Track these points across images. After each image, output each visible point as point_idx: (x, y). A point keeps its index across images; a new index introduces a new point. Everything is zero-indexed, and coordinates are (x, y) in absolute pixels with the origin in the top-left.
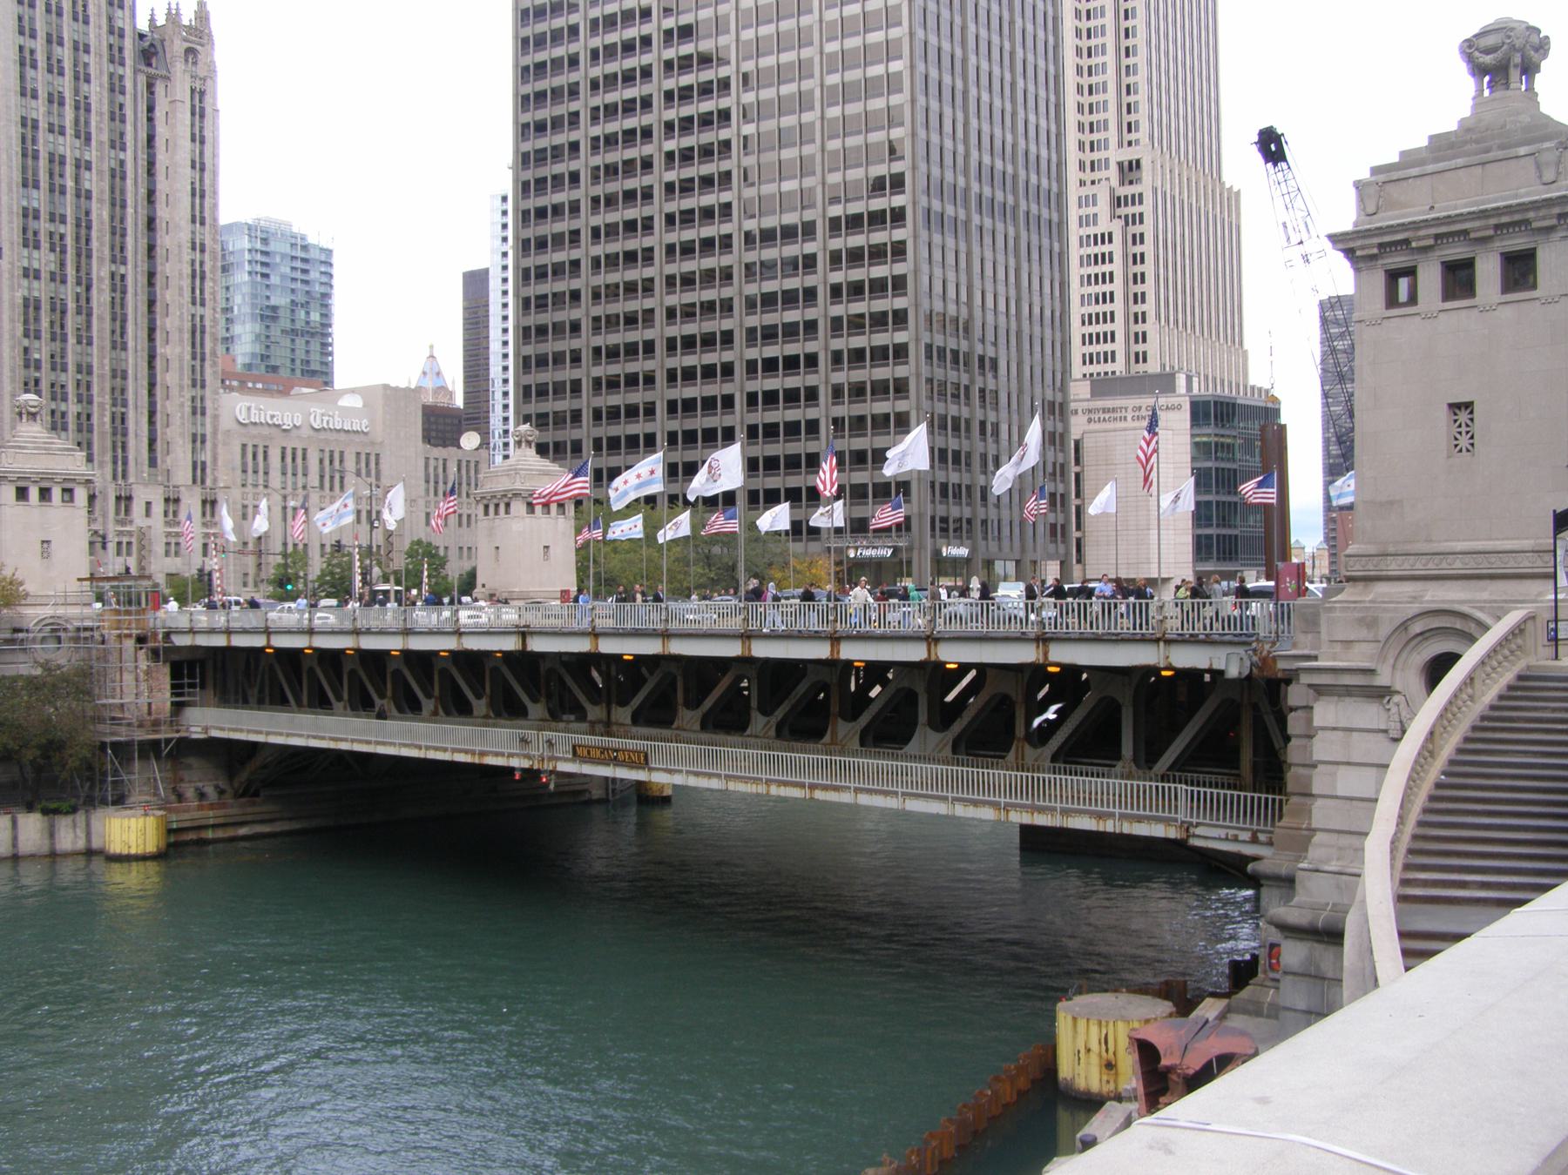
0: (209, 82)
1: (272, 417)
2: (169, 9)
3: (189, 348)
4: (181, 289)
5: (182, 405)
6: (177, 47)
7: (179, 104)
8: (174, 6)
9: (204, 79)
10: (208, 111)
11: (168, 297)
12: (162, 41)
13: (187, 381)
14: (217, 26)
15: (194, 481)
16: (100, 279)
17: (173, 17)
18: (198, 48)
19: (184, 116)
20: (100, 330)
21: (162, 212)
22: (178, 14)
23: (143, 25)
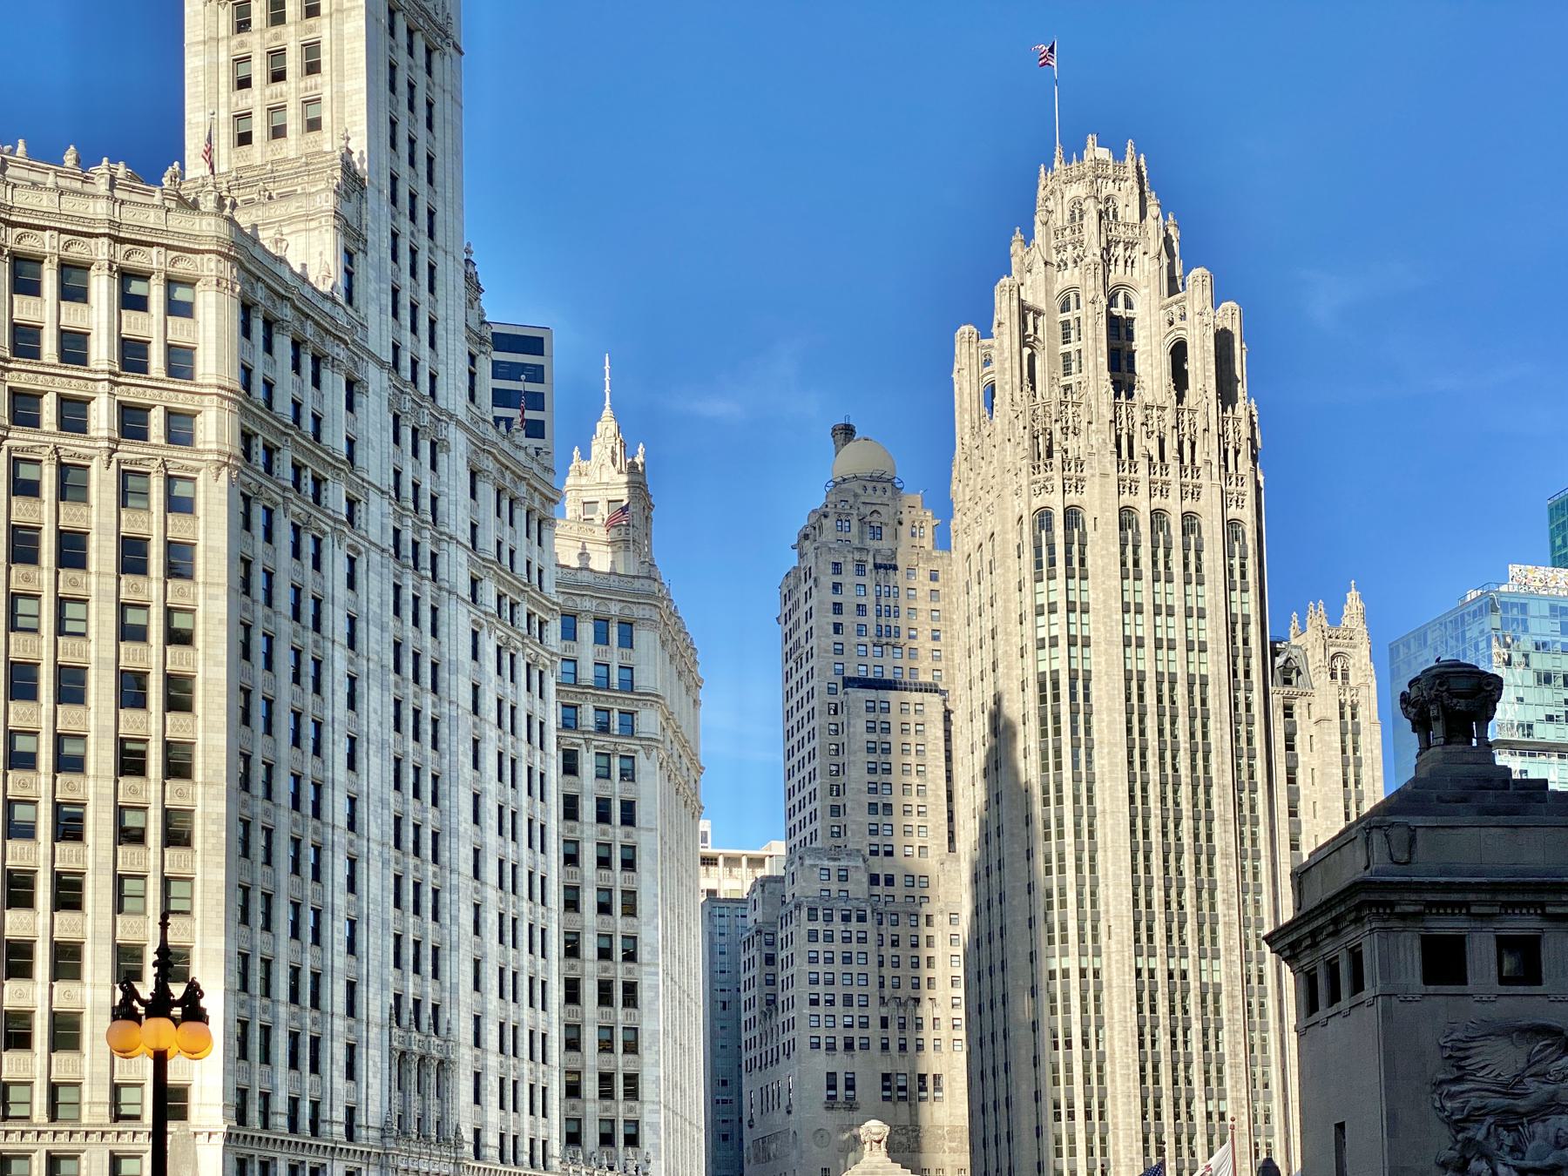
18: (1349, 650)
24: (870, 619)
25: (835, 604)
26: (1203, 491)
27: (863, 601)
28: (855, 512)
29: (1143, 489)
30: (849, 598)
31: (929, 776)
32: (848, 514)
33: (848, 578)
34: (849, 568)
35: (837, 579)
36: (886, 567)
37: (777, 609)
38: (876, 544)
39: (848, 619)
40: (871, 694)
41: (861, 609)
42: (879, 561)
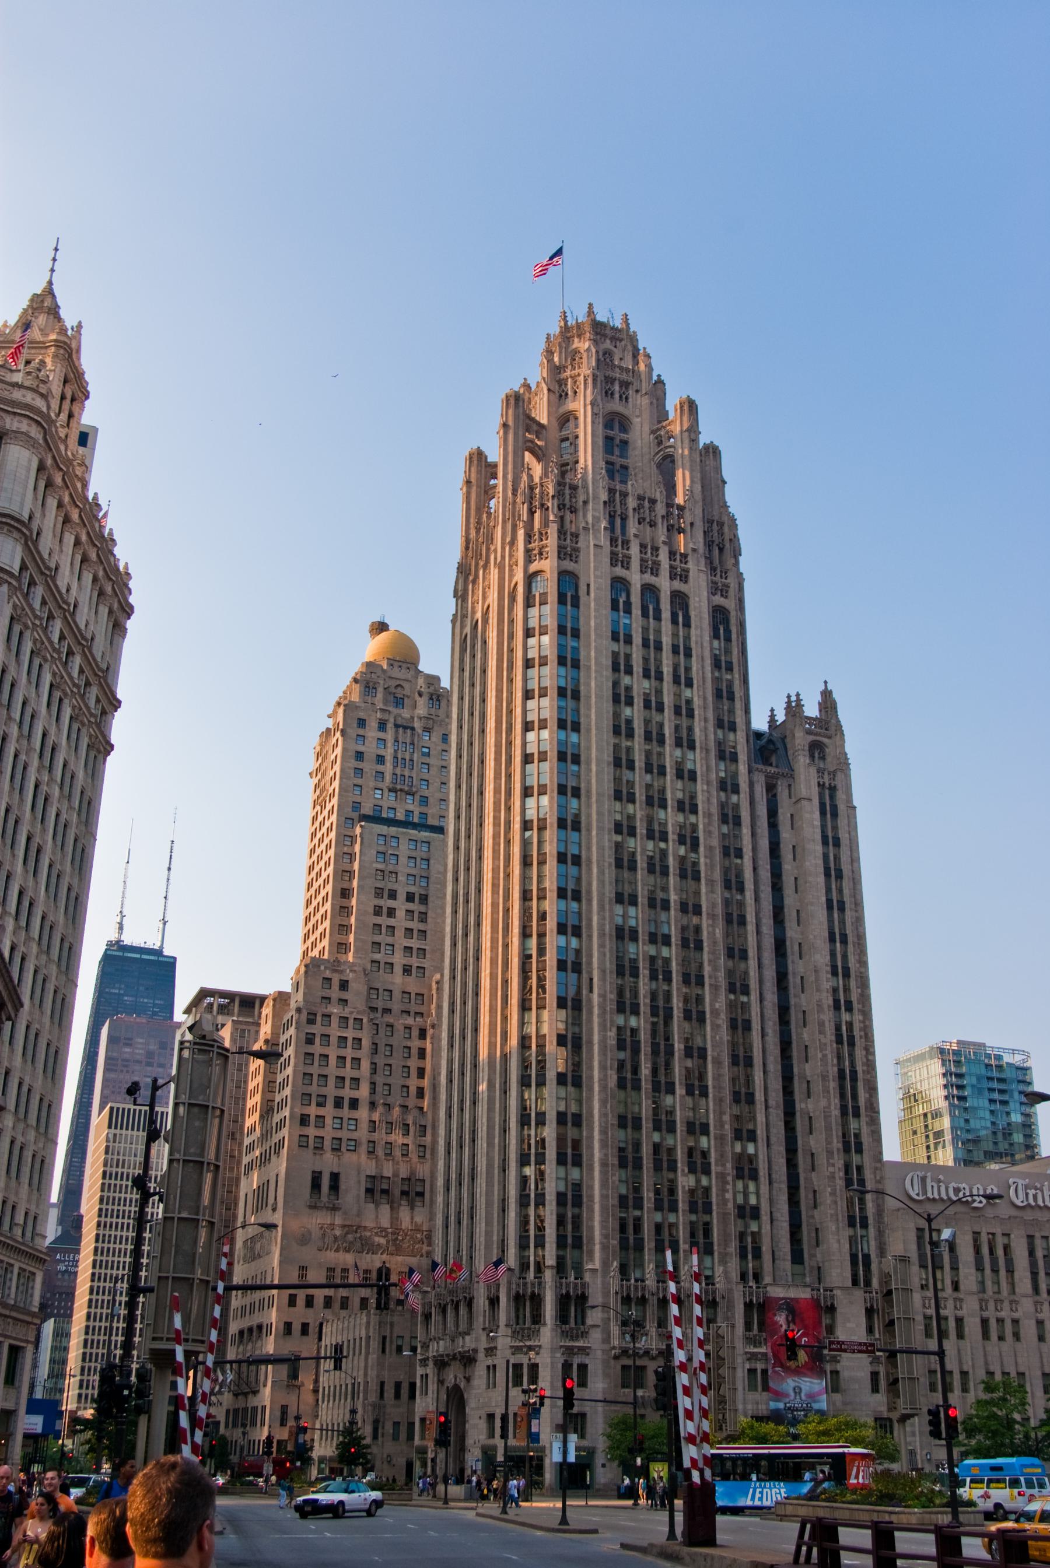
0: (840, 776)
1: (957, 1190)
2: (789, 702)
3: (837, 1101)
4: (821, 1024)
5: (832, 1177)
6: (800, 740)
7: (805, 803)
8: (793, 698)
9: (833, 774)
10: (842, 807)
11: (805, 1036)
12: (783, 739)
13: (837, 1144)
14: (845, 715)
15: (855, 1282)
16: (715, 1013)
17: (794, 708)
18: (825, 740)
19: (811, 815)
20: (717, 1077)
21: (792, 932)
22: (799, 704)
23: (760, 723)
24: (388, 768)
25: (357, 752)
26: (691, 574)
27: (382, 752)
28: (382, 682)
29: (635, 564)
30: (370, 748)
31: (430, 905)
32: (375, 683)
33: (372, 732)
34: (372, 724)
35: (361, 732)
36: (405, 728)
37: (312, 765)
38: (395, 711)
39: (368, 766)
40: (384, 829)
41: (381, 759)
42: (399, 722)
